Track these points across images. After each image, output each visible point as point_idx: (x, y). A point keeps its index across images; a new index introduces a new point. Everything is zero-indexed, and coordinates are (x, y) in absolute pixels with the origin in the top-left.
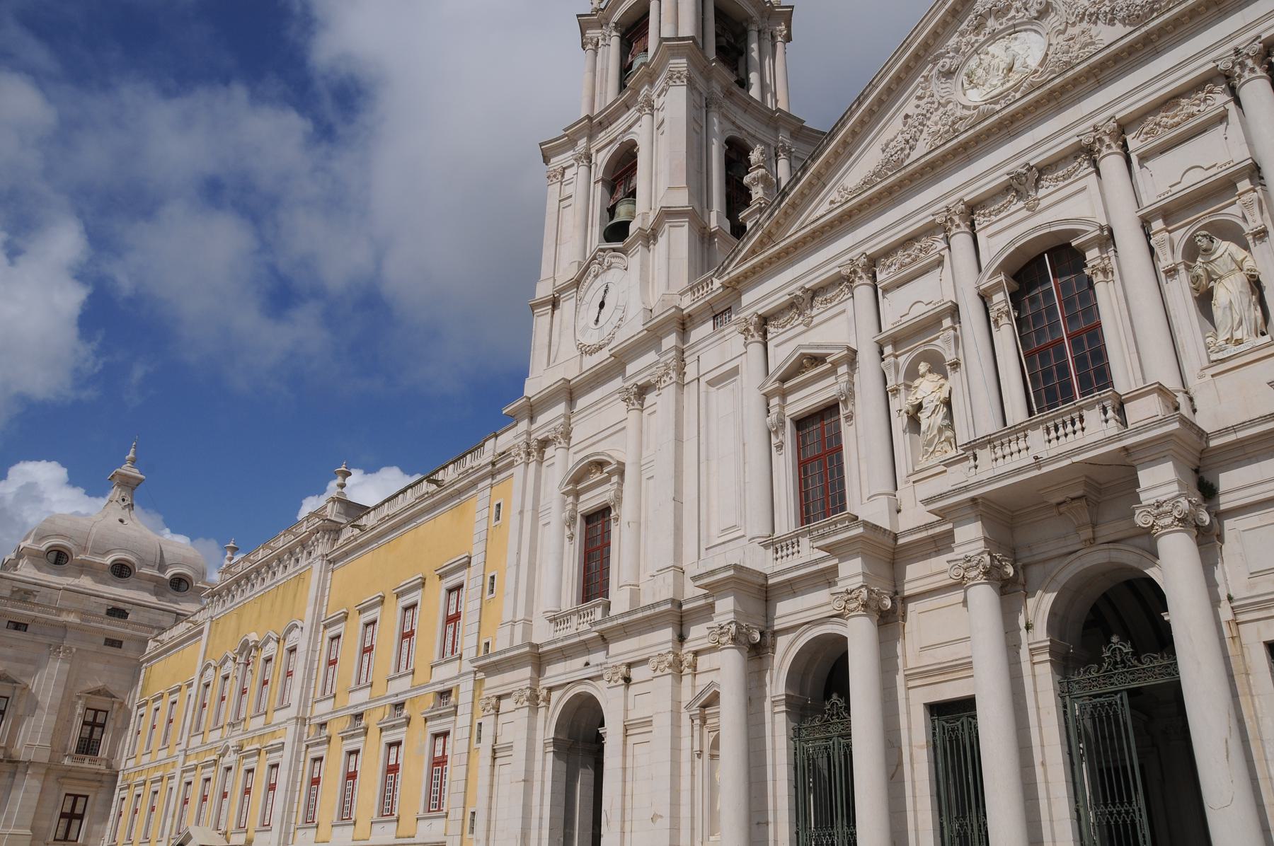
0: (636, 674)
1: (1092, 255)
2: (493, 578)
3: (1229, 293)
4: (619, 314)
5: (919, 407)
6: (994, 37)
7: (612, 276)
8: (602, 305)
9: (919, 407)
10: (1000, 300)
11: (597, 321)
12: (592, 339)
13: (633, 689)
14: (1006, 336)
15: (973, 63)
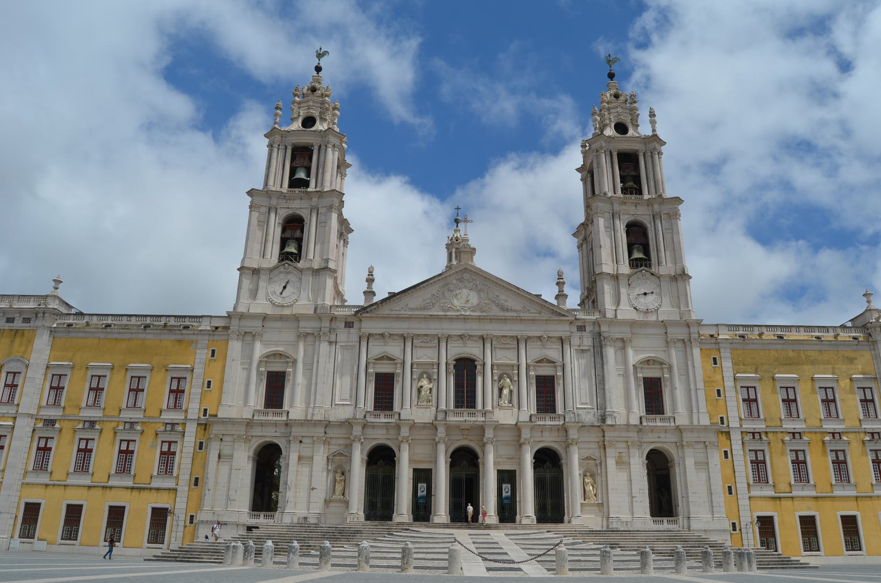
0: (304, 440)
1: (479, 367)
2: (209, 382)
3: (506, 392)
4: (294, 297)
5: (421, 387)
6: (466, 287)
7: (290, 277)
8: (285, 287)
9: (421, 387)
10: (452, 367)
11: (281, 293)
12: (278, 300)
13: (302, 445)
14: (452, 379)
15: (458, 292)
